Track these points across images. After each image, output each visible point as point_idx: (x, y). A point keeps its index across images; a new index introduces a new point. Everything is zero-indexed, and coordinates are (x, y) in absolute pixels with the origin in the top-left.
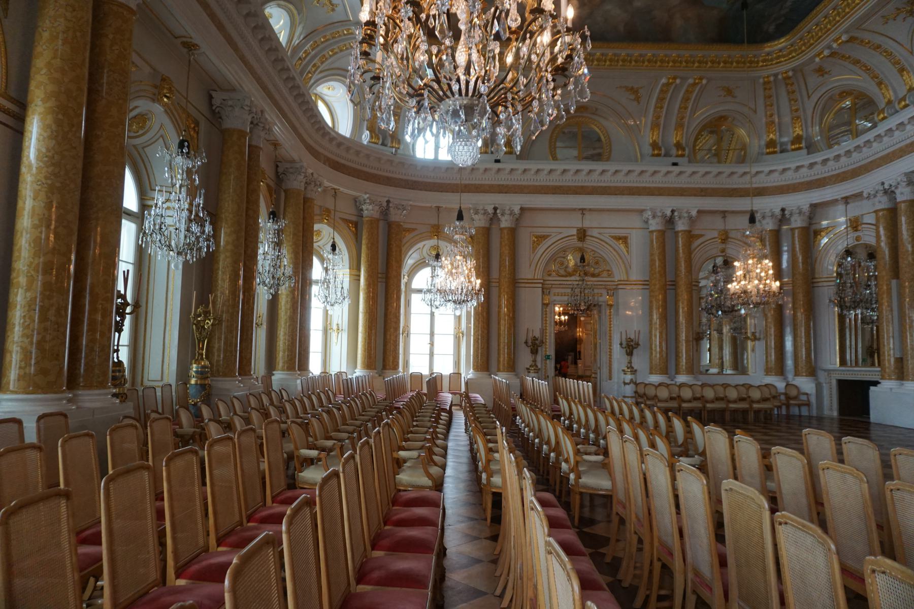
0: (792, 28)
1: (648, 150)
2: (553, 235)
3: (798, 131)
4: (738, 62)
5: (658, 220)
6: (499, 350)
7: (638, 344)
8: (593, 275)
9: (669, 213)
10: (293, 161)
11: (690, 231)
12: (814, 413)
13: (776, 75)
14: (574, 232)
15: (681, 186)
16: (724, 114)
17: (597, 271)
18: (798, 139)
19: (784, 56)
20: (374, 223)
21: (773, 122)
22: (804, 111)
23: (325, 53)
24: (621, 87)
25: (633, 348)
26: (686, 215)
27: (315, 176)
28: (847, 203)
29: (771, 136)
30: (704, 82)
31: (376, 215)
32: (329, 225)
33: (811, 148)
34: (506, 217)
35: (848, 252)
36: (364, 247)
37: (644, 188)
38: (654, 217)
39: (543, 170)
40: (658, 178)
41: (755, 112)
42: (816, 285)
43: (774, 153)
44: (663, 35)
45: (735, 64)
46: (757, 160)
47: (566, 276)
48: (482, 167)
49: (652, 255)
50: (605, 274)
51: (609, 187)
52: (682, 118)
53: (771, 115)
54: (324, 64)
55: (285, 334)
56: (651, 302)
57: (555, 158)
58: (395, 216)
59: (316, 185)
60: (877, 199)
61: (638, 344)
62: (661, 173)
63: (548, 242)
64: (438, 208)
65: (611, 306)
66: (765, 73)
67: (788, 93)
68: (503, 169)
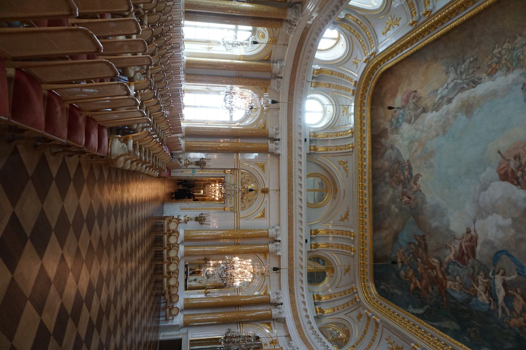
0: (382, 296)
1: (314, 228)
2: (265, 175)
3: (326, 312)
4: (364, 271)
5: (275, 233)
6: (199, 142)
7: (202, 224)
8: (242, 198)
9: (278, 239)
10: (302, 11)
11: (268, 252)
12: (161, 324)
13: (357, 292)
14: (267, 187)
15: (294, 246)
16: (335, 271)
17: (244, 201)
18: (322, 311)
19: (367, 295)
20: (269, 70)
21: (331, 297)
22: (337, 314)
23: (361, 36)
24: (348, 208)
25: (199, 221)
26: (277, 249)
27: (295, 28)
28: (286, 336)
29: (323, 298)
30: (353, 253)
31: (274, 71)
32: (268, 41)
33: (317, 318)
34: (274, 146)
35: (258, 338)
36: (256, 63)
37: (292, 225)
38: (276, 230)
39: (302, 166)
40: (299, 232)
41: (337, 288)
42: (238, 325)
43: (314, 299)
44: (377, 227)
45: (362, 269)
46: (310, 291)
47: (241, 183)
48: (302, 132)
49: (254, 230)
50: (243, 206)
51: (292, 205)
52: (332, 247)
53: (335, 296)
54: (354, 37)
55: (206, 3)
56: (227, 230)
57: (308, 176)
58: (274, 83)
59: (290, 29)
60: (288, 347)
61: (202, 224)
62: (301, 233)
63: (260, 171)
64: (279, 109)
65: (225, 209)
66: (358, 287)
67: (347, 303)
68: (301, 144)
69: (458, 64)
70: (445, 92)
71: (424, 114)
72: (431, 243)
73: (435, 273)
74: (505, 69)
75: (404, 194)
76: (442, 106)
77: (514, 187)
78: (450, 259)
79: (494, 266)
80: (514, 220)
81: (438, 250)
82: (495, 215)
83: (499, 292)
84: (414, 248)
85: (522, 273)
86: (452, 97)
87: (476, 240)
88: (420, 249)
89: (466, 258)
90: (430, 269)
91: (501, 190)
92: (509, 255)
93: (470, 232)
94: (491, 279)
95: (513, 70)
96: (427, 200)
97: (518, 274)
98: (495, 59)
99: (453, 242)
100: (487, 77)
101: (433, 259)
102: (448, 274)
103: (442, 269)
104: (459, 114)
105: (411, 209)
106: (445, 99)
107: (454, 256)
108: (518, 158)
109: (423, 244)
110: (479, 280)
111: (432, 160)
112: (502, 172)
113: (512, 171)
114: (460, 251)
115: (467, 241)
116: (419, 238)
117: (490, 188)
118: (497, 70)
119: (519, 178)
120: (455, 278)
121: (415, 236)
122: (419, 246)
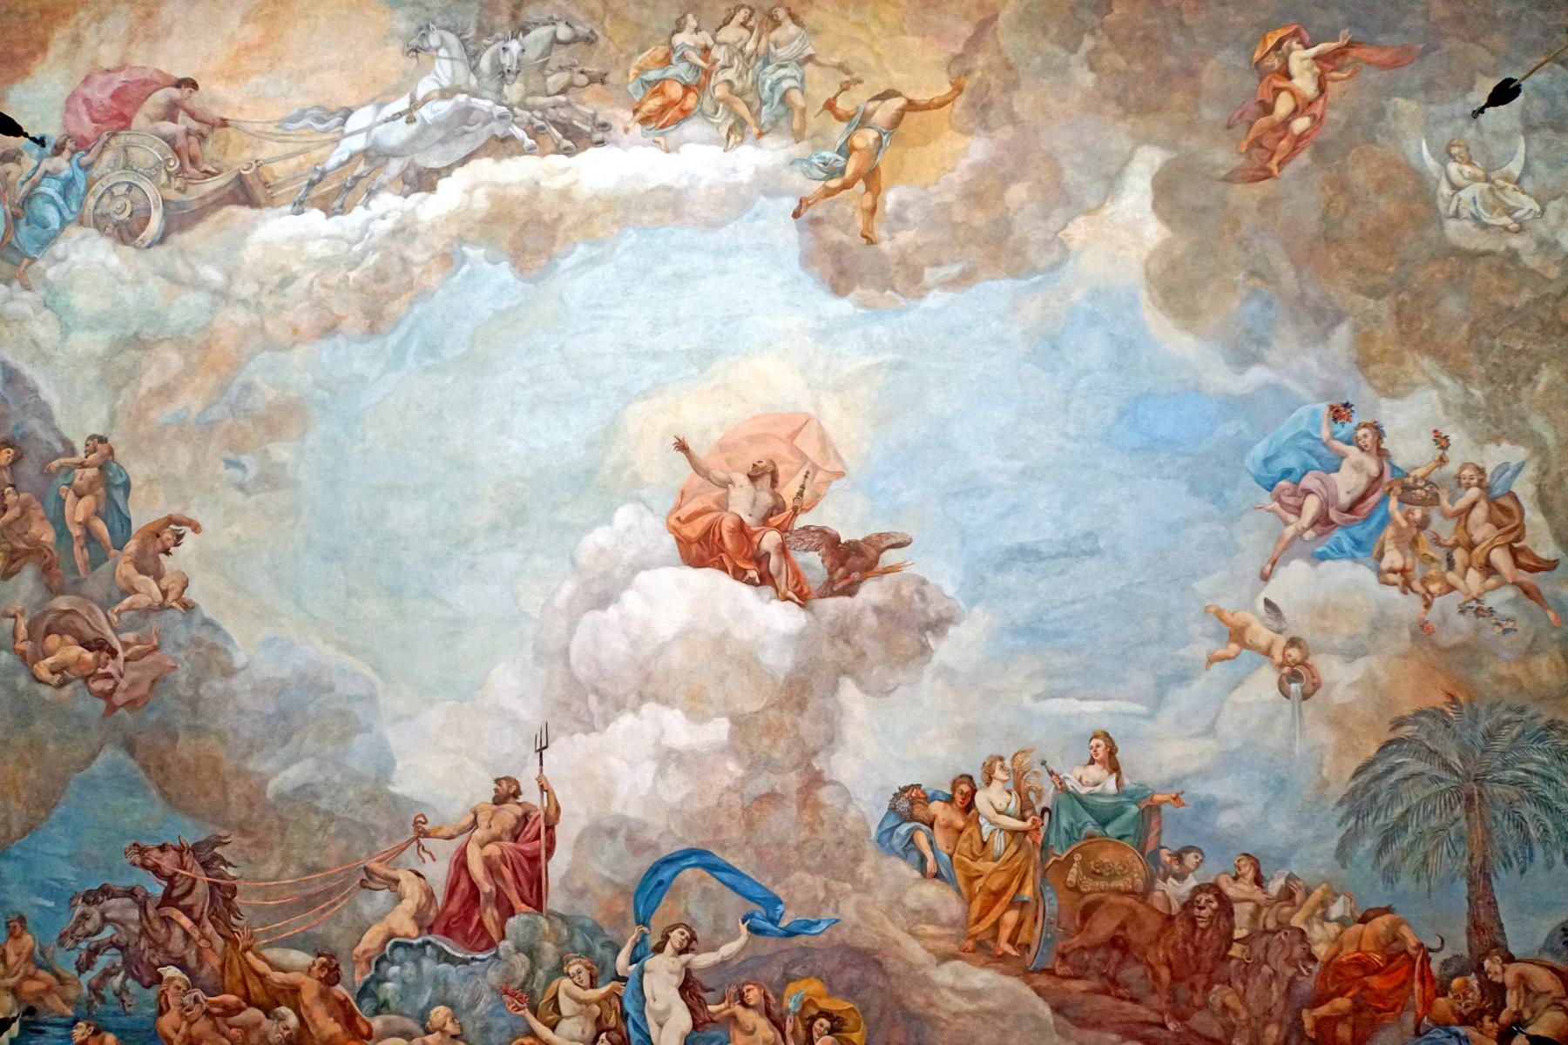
69: (485, 30)
70: (398, 133)
71: (243, 212)
72: (259, 875)
73: (293, 1020)
74: (723, 121)
75: (46, 627)
76: (371, 194)
77: (745, 591)
78: (391, 936)
79: (643, 921)
80: (740, 723)
81: (308, 903)
82: (649, 708)
83: (661, 1026)
84: (135, 914)
85: (768, 925)
86: (435, 164)
87: (550, 828)
88: (176, 913)
89: (490, 915)
90: (250, 1003)
91: (684, 602)
92: (714, 868)
93: (517, 794)
94: (624, 979)
95: (761, 135)
96: (239, 659)
97: (755, 931)
98: (679, 69)
99: (410, 854)
100: (637, 129)
101: (274, 954)
102: (381, 1007)
103: (340, 990)
104: (475, 253)
105: (112, 708)
106: (395, 166)
107: (419, 917)
108: (767, 479)
109: (201, 888)
110: (561, 996)
111: (282, 452)
112: (694, 530)
113: (741, 527)
114: (451, 891)
115: (496, 839)
116: (168, 862)
117: (630, 598)
118: (686, 114)
119: (768, 554)
120: (423, 1017)
121: (142, 851)
122: (168, 900)
